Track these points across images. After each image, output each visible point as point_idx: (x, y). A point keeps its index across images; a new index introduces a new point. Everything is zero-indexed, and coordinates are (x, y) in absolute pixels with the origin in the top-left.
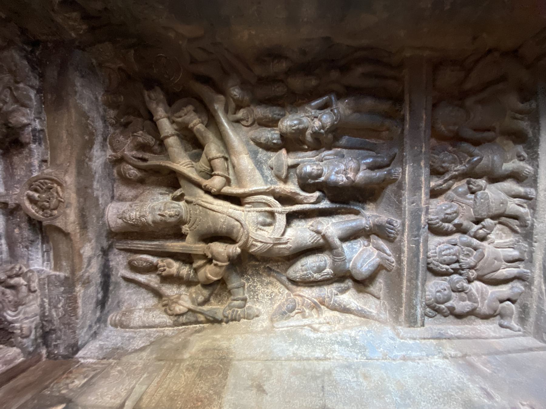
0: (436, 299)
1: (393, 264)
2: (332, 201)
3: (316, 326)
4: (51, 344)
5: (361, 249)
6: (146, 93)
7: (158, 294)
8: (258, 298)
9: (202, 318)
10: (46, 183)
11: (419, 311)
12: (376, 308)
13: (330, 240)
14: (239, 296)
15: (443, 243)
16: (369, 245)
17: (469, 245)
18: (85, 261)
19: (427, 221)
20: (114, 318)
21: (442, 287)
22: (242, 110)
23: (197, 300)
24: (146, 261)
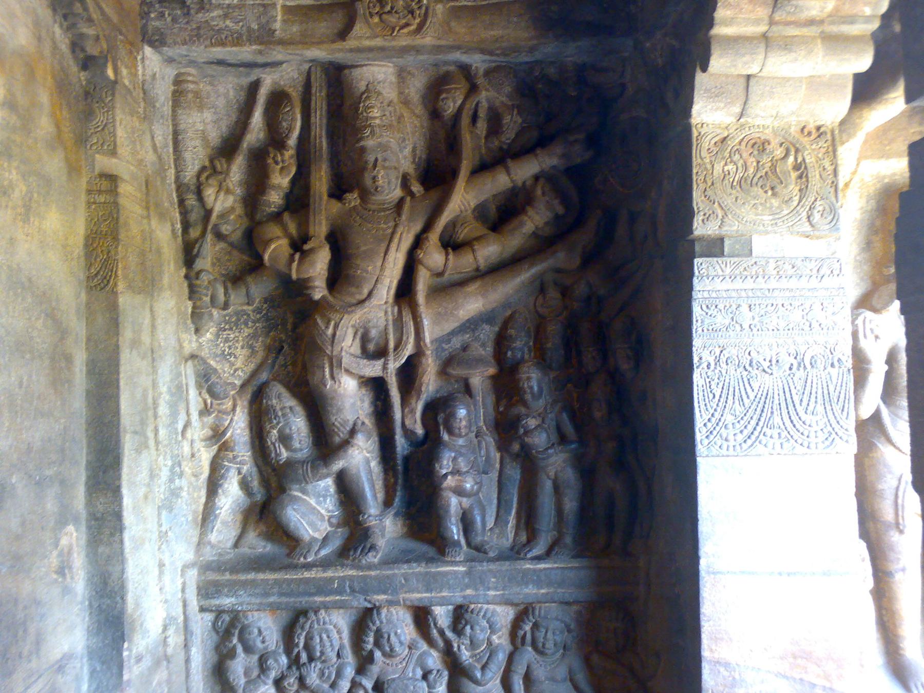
0: (248, 626)
1: (302, 559)
2: (407, 459)
3: (189, 435)
4: (165, 7)
5: (323, 512)
6: (581, 136)
7: (228, 148)
8: (225, 330)
9: (194, 233)
10: (420, 8)
11: (227, 601)
12: (219, 542)
13: (341, 453)
14: (232, 297)
15: (341, 638)
16: (331, 524)
17: (339, 674)
18: (297, 52)
19: (377, 604)
20: (190, 78)
21: (267, 638)
22: (559, 296)
23: (225, 223)
24: (290, 129)
